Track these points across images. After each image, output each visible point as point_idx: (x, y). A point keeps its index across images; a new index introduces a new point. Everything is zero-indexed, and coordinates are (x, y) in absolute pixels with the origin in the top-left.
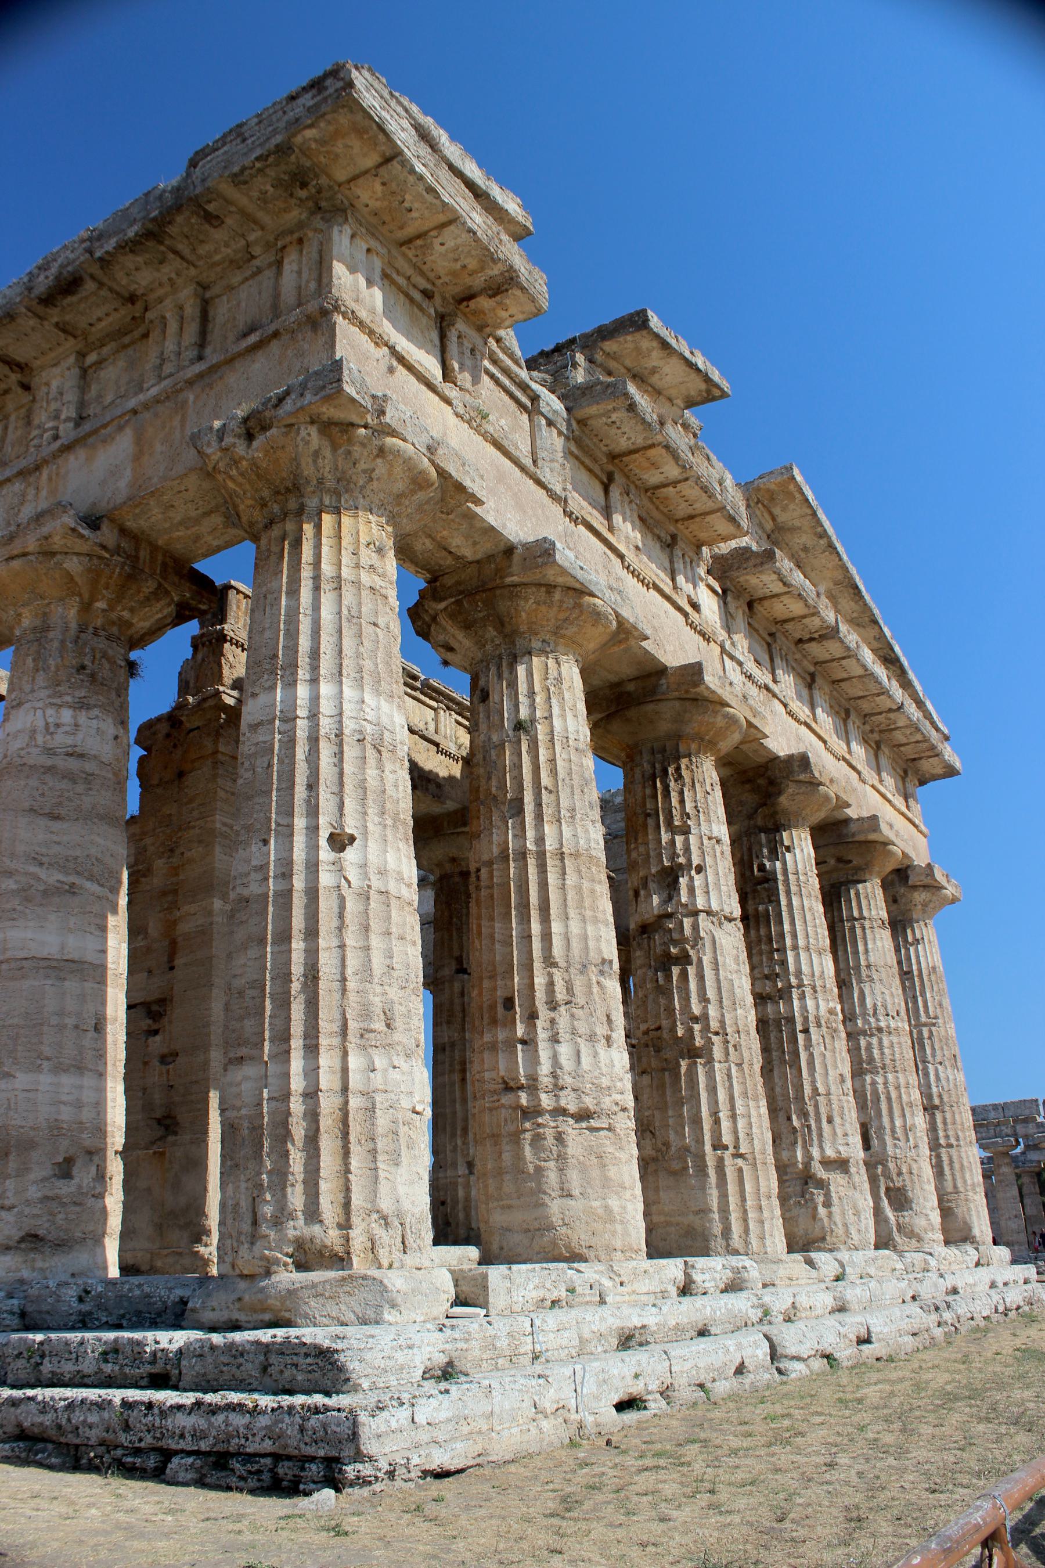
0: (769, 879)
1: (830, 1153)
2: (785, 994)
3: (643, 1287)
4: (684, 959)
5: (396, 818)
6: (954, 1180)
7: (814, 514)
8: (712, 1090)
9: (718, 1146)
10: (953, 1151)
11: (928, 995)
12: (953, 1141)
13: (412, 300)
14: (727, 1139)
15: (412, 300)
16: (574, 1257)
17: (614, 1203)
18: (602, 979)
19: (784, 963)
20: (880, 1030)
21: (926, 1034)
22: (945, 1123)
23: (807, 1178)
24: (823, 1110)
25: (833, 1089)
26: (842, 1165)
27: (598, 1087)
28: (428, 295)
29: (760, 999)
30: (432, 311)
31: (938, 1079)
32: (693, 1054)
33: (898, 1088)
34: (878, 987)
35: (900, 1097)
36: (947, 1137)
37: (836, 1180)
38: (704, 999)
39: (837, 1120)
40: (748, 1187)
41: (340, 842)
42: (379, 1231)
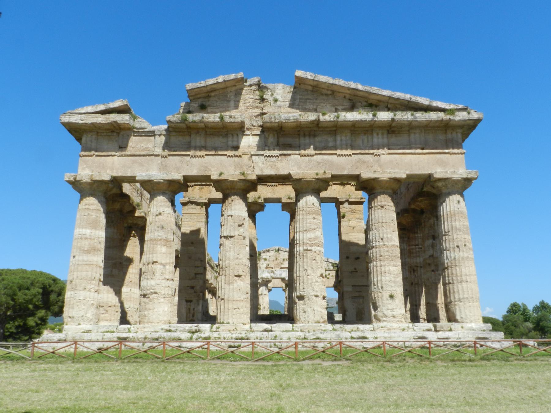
1: (298, 294)
5: (84, 250)
6: (450, 297)
7: (314, 80)
10: (451, 286)
11: (446, 223)
12: (451, 281)
13: (109, 136)
15: (109, 136)
17: (146, 313)
18: (153, 266)
20: (373, 247)
21: (444, 239)
22: (448, 274)
24: (298, 281)
25: (301, 274)
27: (147, 290)
28: (113, 131)
30: (115, 134)
31: (447, 258)
33: (377, 267)
35: (377, 271)
36: (449, 280)
39: (301, 284)
40: (222, 307)
41: (74, 257)
42: (69, 320)
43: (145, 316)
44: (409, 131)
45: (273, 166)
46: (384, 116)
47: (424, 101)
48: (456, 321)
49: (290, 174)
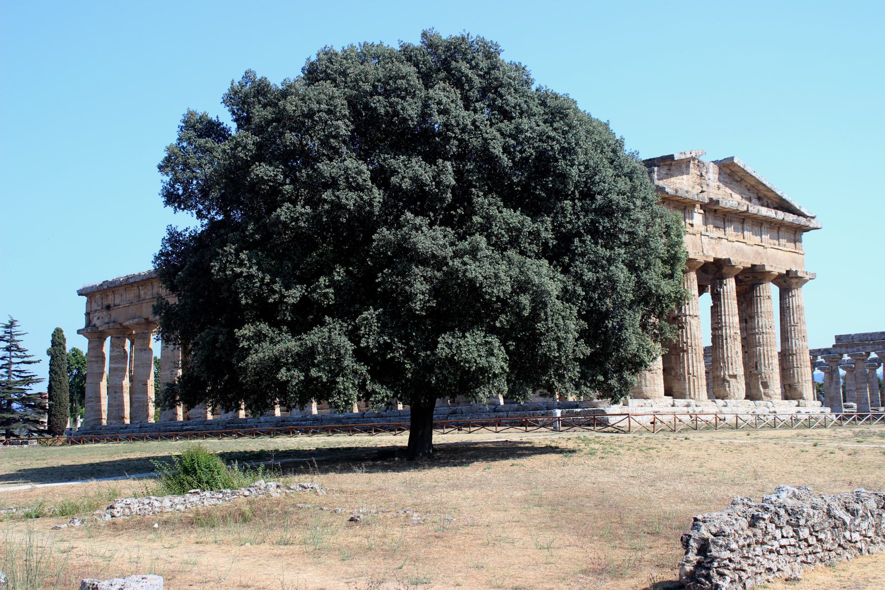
0: (719, 294)
1: (731, 373)
2: (721, 328)
3: (662, 403)
4: (683, 328)
8: (688, 360)
9: (689, 374)
14: (691, 372)
16: (647, 398)
19: (721, 319)
23: (724, 380)
26: (735, 376)
29: (713, 329)
32: (684, 351)
34: (764, 319)
37: (732, 381)
38: (687, 338)
43: (655, 390)
44: (779, 228)
45: (713, 249)
46: (781, 215)
47: (797, 205)
48: (803, 399)
49: (729, 260)
